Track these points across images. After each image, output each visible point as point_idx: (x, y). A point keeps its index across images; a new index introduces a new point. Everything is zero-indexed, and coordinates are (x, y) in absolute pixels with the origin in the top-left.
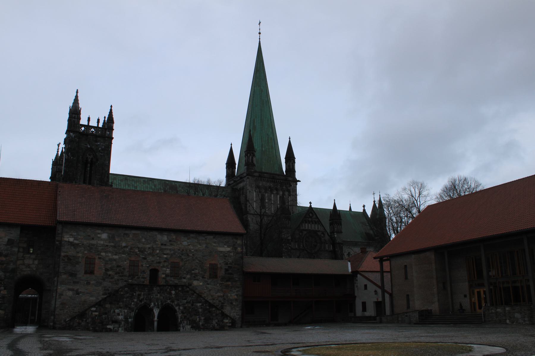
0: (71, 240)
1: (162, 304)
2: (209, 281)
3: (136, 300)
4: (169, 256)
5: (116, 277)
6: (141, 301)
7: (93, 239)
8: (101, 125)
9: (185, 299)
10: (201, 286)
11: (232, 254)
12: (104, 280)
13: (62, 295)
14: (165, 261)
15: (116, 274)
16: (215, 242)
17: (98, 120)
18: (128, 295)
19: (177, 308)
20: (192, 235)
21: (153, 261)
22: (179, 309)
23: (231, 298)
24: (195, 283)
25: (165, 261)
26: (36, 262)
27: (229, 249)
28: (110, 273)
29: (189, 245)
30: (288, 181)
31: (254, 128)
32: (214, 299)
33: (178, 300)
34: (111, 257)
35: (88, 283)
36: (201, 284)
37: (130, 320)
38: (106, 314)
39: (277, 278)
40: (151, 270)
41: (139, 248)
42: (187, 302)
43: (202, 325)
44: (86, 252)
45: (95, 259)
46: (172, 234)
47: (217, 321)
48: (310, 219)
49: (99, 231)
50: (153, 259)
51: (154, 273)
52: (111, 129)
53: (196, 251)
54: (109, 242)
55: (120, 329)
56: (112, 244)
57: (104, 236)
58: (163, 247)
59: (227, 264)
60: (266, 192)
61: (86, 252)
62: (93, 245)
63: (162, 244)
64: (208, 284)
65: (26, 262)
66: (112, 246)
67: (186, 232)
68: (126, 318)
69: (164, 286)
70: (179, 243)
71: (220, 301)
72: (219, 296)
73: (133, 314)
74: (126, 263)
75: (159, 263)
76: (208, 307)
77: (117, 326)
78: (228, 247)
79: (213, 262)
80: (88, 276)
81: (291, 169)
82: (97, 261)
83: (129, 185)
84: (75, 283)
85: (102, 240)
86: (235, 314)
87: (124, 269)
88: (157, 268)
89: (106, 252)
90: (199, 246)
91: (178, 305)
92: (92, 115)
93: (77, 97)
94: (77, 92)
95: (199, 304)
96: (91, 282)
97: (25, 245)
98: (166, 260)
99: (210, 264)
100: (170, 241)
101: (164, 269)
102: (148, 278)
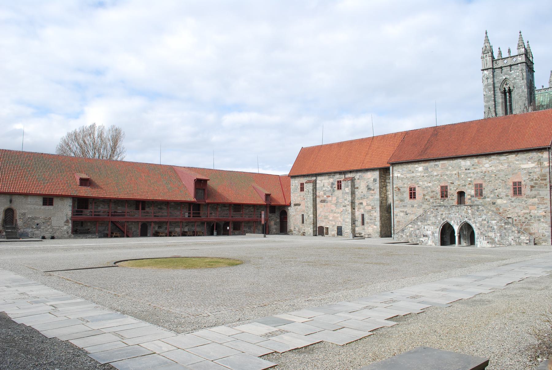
0: (399, 175)
2: (513, 199)
3: (439, 219)
4: (472, 179)
6: (443, 219)
12: (423, 203)
13: (397, 215)
14: (469, 184)
16: (517, 160)
18: (433, 215)
19: (473, 226)
23: (538, 214)
24: (499, 201)
25: (469, 184)
28: (426, 197)
32: (519, 216)
34: (426, 185)
35: (413, 206)
36: (505, 202)
37: (436, 235)
43: (499, 241)
47: (513, 237)
50: (459, 183)
51: (461, 194)
55: (429, 241)
58: (468, 171)
59: (532, 180)
62: (413, 177)
63: (466, 169)
70: (481, 165)
71: (526, 218)
73: (438, 230)
74: (438, 189)
75: (465, 186)
76: (503, 224)
77: (427, 238)
78: (532, 163)
79: (517, 180)
80: (412, 200)
82: (417, 189)
86: (544, 231)
87: (437, 193)
89: (422, 181)
94: (486, 33)
95: (494, 222)
96: (415, 205)
100: (473, 165)
101: (469, 191)
102: (456, 200)
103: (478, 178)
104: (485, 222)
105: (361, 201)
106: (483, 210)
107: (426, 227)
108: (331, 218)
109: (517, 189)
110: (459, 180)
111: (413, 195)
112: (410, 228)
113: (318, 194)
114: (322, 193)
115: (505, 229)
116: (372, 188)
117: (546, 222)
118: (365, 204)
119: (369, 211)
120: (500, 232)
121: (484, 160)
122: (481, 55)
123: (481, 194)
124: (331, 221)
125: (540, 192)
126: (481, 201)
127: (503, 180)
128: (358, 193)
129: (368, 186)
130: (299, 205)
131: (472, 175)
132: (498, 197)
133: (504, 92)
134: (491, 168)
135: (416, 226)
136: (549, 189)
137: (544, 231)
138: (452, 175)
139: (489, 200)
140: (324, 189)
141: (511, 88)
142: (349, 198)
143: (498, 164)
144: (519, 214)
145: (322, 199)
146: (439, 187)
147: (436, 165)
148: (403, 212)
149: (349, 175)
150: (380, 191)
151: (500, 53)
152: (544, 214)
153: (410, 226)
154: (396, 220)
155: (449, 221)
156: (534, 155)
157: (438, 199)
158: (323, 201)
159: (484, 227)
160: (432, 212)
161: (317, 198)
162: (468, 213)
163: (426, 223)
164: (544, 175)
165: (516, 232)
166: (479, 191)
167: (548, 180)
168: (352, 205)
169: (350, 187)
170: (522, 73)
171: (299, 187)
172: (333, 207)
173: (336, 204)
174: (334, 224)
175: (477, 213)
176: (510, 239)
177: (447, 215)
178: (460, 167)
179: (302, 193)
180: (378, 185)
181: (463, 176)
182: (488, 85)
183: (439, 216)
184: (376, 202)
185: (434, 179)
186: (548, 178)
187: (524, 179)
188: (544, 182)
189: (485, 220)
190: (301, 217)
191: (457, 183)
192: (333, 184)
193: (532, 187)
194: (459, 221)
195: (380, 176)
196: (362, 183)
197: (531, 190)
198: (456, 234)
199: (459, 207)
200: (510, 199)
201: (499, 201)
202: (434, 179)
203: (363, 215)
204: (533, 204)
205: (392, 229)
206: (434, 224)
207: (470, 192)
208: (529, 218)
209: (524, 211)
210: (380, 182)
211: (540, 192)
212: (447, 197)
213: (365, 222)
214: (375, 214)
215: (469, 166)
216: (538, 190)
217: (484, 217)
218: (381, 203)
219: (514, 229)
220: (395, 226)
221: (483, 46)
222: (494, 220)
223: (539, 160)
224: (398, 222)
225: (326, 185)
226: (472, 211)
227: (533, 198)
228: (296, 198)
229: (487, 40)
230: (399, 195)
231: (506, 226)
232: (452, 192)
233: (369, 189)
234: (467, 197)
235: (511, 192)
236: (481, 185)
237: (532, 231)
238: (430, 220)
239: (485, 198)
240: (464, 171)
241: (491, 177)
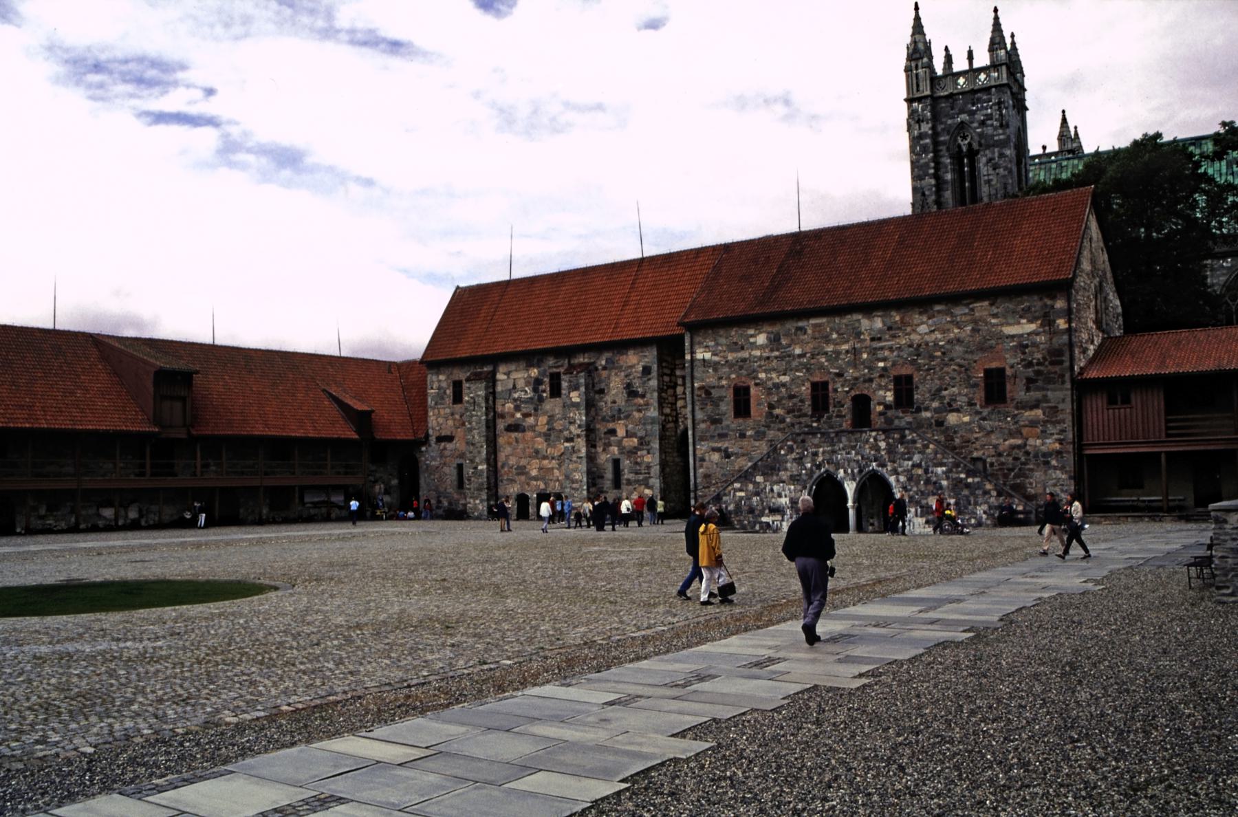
0: (708, 356)
1: (860, 471)
2: (985, 412)
4: (889, 364)
5: (788, 420)
6: (819, 467)
7: (742, 348)
9: (909, 459)
10: (966, 423)
12: (768, 427)
13: (703, 460)
14: (881, 376)
15: (788, 413)
16: (995, 316)
18: (793, 456)
19: (892, 479)
20: (937, 308)
21: (856, 379)
22: (898, 481)
24: (952, 418)
25: (881, 376)
28: (777, 411)
29: (933, 331)
32: (1000, 455)
33: (894, 462)
35: (743, 436)
36: (967, 419)
38: (757, 494)
40: (855, 399)
41: (826, 353)
42: (913, 466)
44: (733, 376)
46: (894, 313)
47: (985, 507)
49: (751, 332)
50: (857, 374)
51: (862, 405)
53: (950, 342)
54: (772, 350)
56: (777, 353)
57: (761, 339)
59: (1030, 364)
61: (733, 376)
62: (744, 360)
63: (873, 339)
64: (984, 419)
66: (776, 357)
67: (923, 304)
68: (794, 502)
70: (909, 329)
71: (1016, 459)
72: (1013, 447)
74: (805, 389)
75: (871, 380)
77: (779, 518)
78: (1030, 321)
79: (994, 365)
80: (741, 420)
82: (753, 391)
84: (722, 436)
87: (802, 401)
88: (865, 392)
89: (766, 371)
90: (956, 331)
91: (895, 472)
92: (960, 43)
93: (917, 18)
94: (917, 8)
95: (940, 470)
96: (749, 433)
98: (884, 373)
101: (881, 393)
102: (849, 417)
103: (901, 361)
104: (920, 472)
105: (611, 426)
106: (914, 442)
107: (775, 488)
108: (534, 473)
109: (995, 387)
110: (855, 367)
111: (742, 406)
112: (736, 490)
114: (510, 406)
115: (968, 486)
117: (1062, 468)
118: (621, 432)
119: (632, 452)
120: (956, 496)
122: (902, 62)
124: (536, 479)
125: (1049, 393)
126: (909, 419)
127: (960, 366)
128: (605, 405)
130: (450, 439)
131: (887, 353)
132: (950, 407)
133: (957, 157)
134: (933, 337)
135: (751, 487)
136: (1068, 385)
137: (1057, 489)
138: (838, 353)
139: (928, 414)
140: (516, 395)
141: (975, 146)
142: (581, 417)
143: (948, 326)
144: (1001, 448)
145: (510, 421)
146: (808, 385)
149: (581, 359)
150: (660, 397)
151: (949, 59)
152: (1057, 446)
153: (737, 485)
155: (832, 469)
156: (1036, 303)
157: (805, 415)
158: (514, 428)
159: (918, 483)
160: (791, 450)
162: (878, 449)
163: (775, 478)
165: (994, 493)
167: (1067, 364)
168: (587, 436)
169: (583, 389)
170: (1000, 109)
172: (540, 444)
173: (547, 436)
175: (901, 449)
176: (980, 510)
177: (827, 456)
178: (859, 334)
179: (458, 407)
180: (654, 383)
181: (865, 356)
182: (922, 136)
183: (809, 459)
184: (649, 427)
185: (795, 364)
186: (1066, 358)
187: (1010, 361)
188: (1057, 369)
189: (919, 466)
190: (455, 472)
192: (538, 381)
193: (1030, 381)
194: (856, 471)
195: (660, 361)
196: (613, 378)
197: (1028, 389)
198: (850, 504)
199: (858, 435)
200: (978, 413)
202: (795, 364)
203: (616, 463)
204: (1033, 423)
205: (692, 495)
206: (794, 479)
208: (1023, 459)
209: (1012, 441)
210: (661, 375)
211: (1049, 393)
212: (826, 409)
214: (648, 459)
215: (880, 331)
216: (1044, 389)
217: (917, 458)
218: (664, 428)
219: (988, 486)
221: (908, 40)
222: (941, 465)
223: (1046, 315)
224: (707, 476)
225: (521, 384)
226: (888, 444)
227: (1032, 408)
228: (440, 420)
229: (918, 27)
230: (709, 407)
231: (970, 480)
232: (839, 396)
235: (979, 395)
236: (909, 378)
237: (1031, 491)
238: (786, 469)
239: (919, 410)
240: (868, 343)
241: (932, 358)
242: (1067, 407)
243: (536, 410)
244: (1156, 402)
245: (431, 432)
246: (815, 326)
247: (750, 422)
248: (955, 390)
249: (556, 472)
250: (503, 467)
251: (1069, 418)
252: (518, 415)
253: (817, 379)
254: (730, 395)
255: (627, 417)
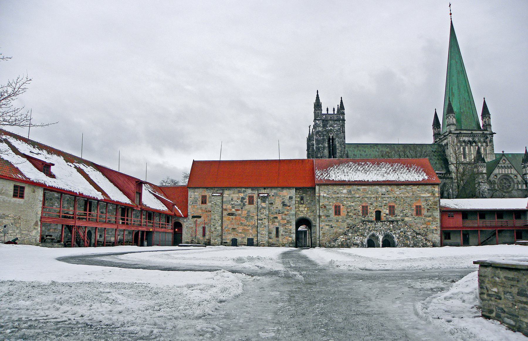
0: (325, 195)
2: (416, 217)
8: (336, 113)
11: (431, 198)
16: (419, 191)
17: (334, 109)
19: (394, 236)
20: (402, 187)
23: (432, 228)
24: (406, 219)
26: (306, 209)
27: (429, 195)
28: (350, 214)
30: (486, 134)
31: (453, 94)
35: (337, 221)
36: (411, 219)
38: (349, 239)
39: (466, 214)
40: (376, 212)
45: (340, 206)
48: (503, 165)
51: (378, 213)
52: (343, 114)
57: (345, 191)
58: (383, 196)
60: (466, 146)
65: (301, 209)
69: (385, 221)
74: (360, 208)
75: (381, 206)
79: (418, 204)
80: (337, 216)
81: (487, 125)
82: (342, 207)
83: (360, 151)
85: (343, 194)
92: (329, 105)
93: (318, 95)
94: (317, 92)
95: (409, 233)
97: (299, 199)
99: (416, 206)
105: (275, 216)
108: (240, 231)
109: (419, 211)
111: (337, 211)
113: (224, 207)
114: (229, 206)
116: (288, 204)
118: (279, 218)
119: (284, 225)
121: (395, 188)
123: (394, 214)
124: (241, 233)
129: (283, 202)
130: (199, 217)
132: (406, 215)
134: (401, 195)
136: (439, 211)
138: (371, 198)
139: (399, 217)
140: (233, 203)
145: (229, 212)
147: (358, 189)
148: (329, 225)
154: (321, 232)
155: (375, 232)
156: (429, 188)
161: (224, 212)
164: (436, 202)
166: (392, 210)
171: (200, 199)
174: (244, 236)
179: (204, 205)
180: (294, 202)
184: (291, 217)
185: (356, 200)
187: (423, 204)
188: (436, 207)
189: (402, 232)
190: (202, 229)
191: (375, 204)
193: (428, 209)
201: (406, 219)
202: (356, 200)
203: (277, 229)
204: (429, 221)
207: (385, 211)
209: (423, 226)
212: (367, 214)
213: (280, 234)
220: (321, 237)
223: (433, 192)
230: (325, 212)
232: (371, 211)
233: (284, 205)
234: (383, 215)
236: (394, 206)
239: (396, 216)
240: (381, 195)
241: (400, 201)
242: (438, 217)
243: (242, 208)
244: (459, 218)
245: (189, 214)
246: (363, 189)
247: (340, 217)
248: (407, 211)
249: (251, 231)
250: (225, 228)
251: (439, 220)
252: (234, 210)
253: (364, 205)
254: (333, 208)
255: (282, 213)
